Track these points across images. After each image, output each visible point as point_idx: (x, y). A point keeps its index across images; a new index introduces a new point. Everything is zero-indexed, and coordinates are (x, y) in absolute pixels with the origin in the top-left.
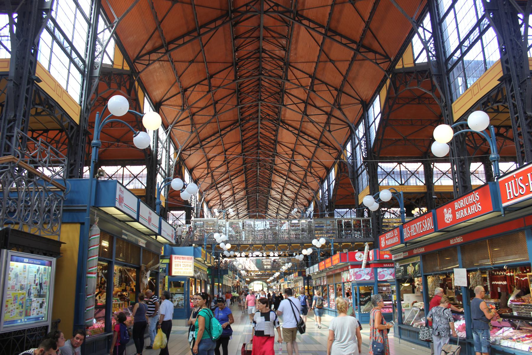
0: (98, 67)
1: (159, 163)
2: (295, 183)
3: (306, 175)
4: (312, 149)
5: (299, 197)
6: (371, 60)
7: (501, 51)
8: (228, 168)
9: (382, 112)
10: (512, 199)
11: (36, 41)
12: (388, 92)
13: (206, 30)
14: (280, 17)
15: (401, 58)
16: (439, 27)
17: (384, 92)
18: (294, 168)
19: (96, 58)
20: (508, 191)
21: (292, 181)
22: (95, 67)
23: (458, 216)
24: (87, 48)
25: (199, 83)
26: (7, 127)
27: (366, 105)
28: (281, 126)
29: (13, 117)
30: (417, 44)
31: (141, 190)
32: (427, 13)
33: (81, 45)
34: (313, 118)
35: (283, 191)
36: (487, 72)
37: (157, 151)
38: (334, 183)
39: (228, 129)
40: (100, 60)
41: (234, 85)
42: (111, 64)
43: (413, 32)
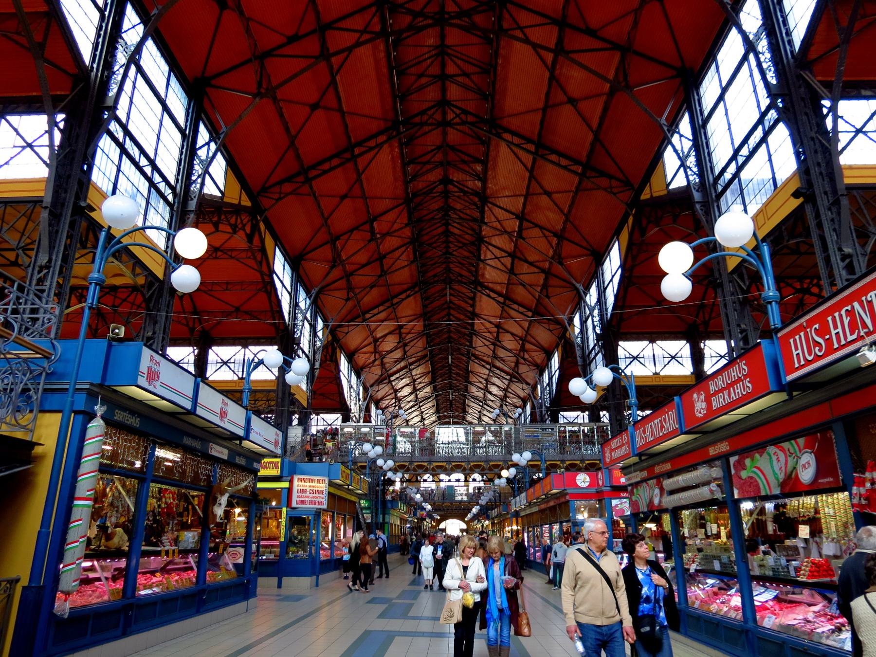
0: (195, 197)
2: (502, 374)
3: (517, 363)
4: (526, 325)
5: (508, 394)
6: (605, 189)
7: (797, 155)
8: (405, 353)
9: (623, 266)
10: (801, 367)
11: (90, 151)
12: (631, 235)
14: (471, 129)
15: (648, 184)
16: (702, 131)
17: (625, 235)
18: (501, 353)
19: (192, 184)
20: (795, 353)
21: (498, 372)
22: (191, 197)
23: (715, 405)
24: (179, 170)
25: (356, 228)
26: (36, 277)
27: (600, 257)
28: (479, 291)
29: (47, 262)
30: (670, 160)
31: (271, 381)
32: (684, 111)
33: (169, 163)
34: (525, 278)
35: (486, 387)
36: (777, 190)
37: (295, 325)
38: (557, 373)
39: (403, 296)
40: (198, 186)
41: (407, 232)
42: (220, 195)
43: (666, 141)
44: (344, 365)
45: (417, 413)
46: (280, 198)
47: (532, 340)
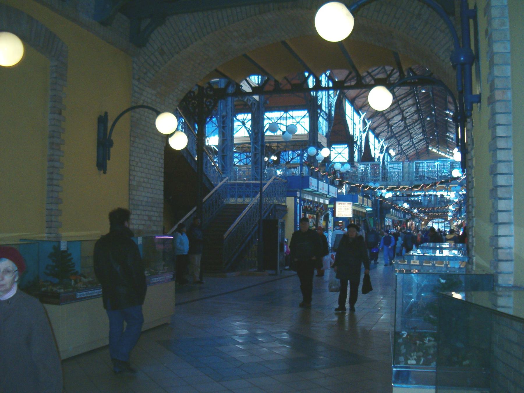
1: (320, 107)
31: (304, 135)
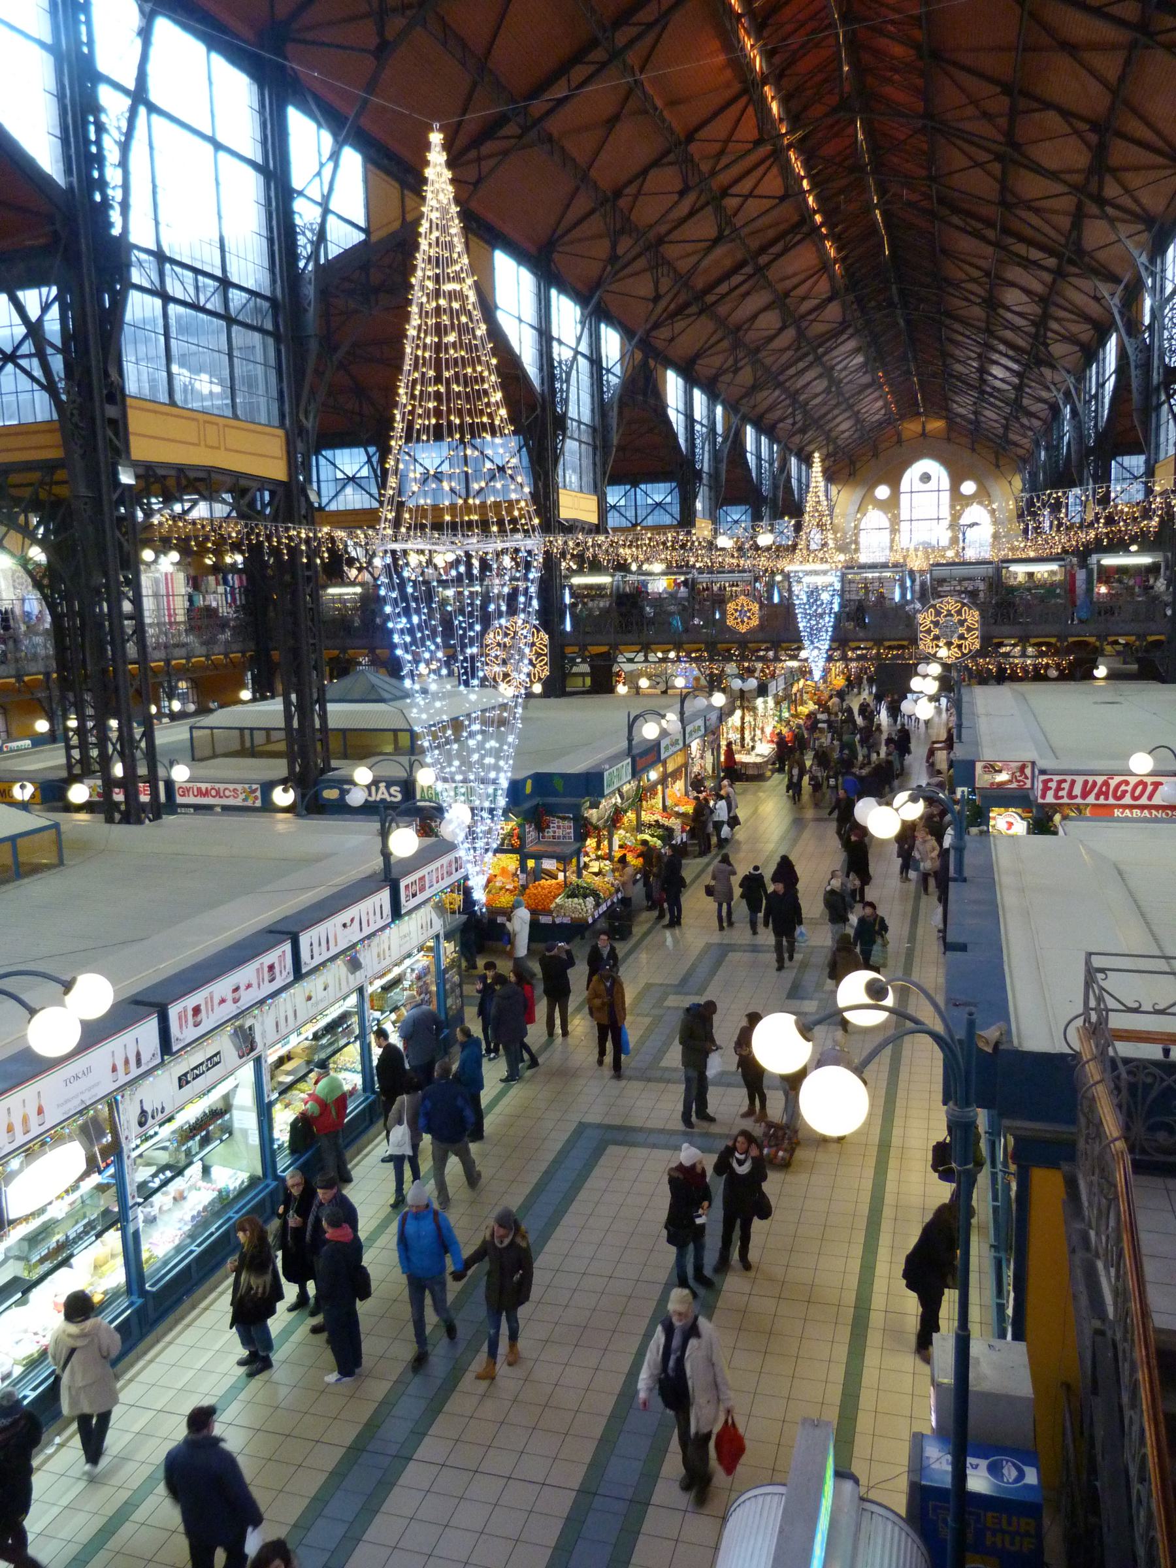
1: (560, 422)
8: (801, 333)
13: (633, 31)
25: (656, 163)
42: (362, 236)
44: (673, 384)
45: (847, 414)
46: (479, 181)
47: (1067, 305)
